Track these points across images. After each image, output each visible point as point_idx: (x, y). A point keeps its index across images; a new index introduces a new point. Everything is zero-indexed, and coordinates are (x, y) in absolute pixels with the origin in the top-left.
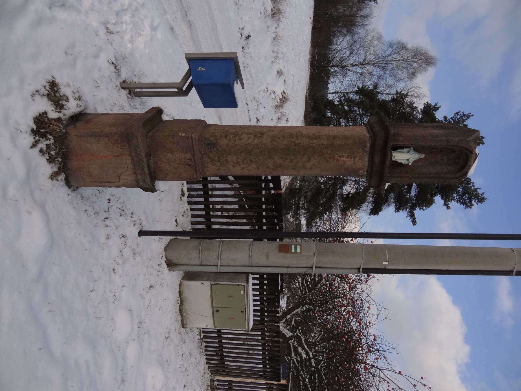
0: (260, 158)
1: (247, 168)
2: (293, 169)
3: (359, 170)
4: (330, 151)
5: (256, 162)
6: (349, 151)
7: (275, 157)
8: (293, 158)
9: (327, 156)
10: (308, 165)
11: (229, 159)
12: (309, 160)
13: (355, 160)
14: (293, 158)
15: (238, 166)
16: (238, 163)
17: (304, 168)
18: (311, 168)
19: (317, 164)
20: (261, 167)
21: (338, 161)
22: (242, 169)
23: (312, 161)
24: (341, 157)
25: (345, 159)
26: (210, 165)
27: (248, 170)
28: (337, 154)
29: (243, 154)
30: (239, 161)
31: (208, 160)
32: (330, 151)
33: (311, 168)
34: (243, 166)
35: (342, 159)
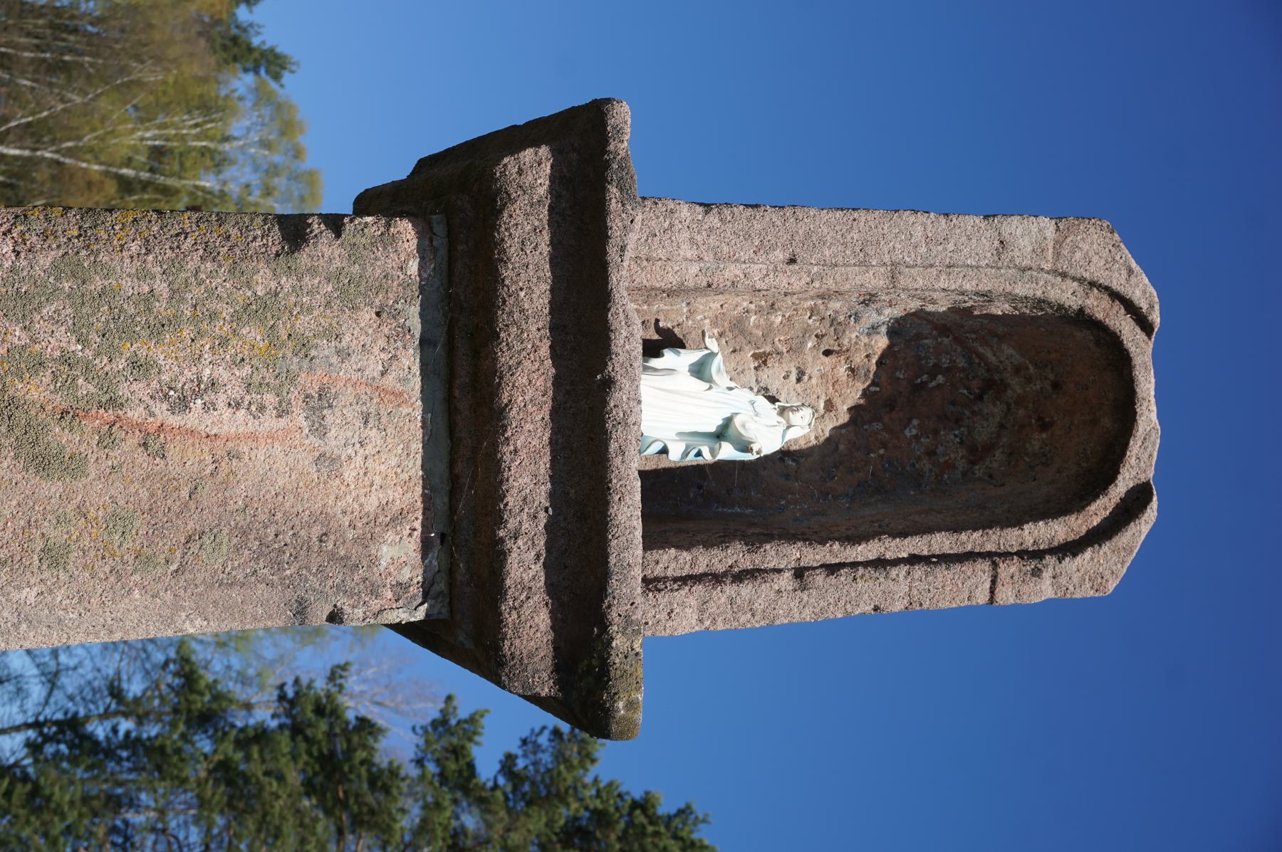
4: (59, 340)
6: (253, 333)
13: (320, 430)
21: (154, 441)
24: (182, 404)
25: (229, 422)
28: (140, 367)
32: (59, 340)
35: (194, 417)
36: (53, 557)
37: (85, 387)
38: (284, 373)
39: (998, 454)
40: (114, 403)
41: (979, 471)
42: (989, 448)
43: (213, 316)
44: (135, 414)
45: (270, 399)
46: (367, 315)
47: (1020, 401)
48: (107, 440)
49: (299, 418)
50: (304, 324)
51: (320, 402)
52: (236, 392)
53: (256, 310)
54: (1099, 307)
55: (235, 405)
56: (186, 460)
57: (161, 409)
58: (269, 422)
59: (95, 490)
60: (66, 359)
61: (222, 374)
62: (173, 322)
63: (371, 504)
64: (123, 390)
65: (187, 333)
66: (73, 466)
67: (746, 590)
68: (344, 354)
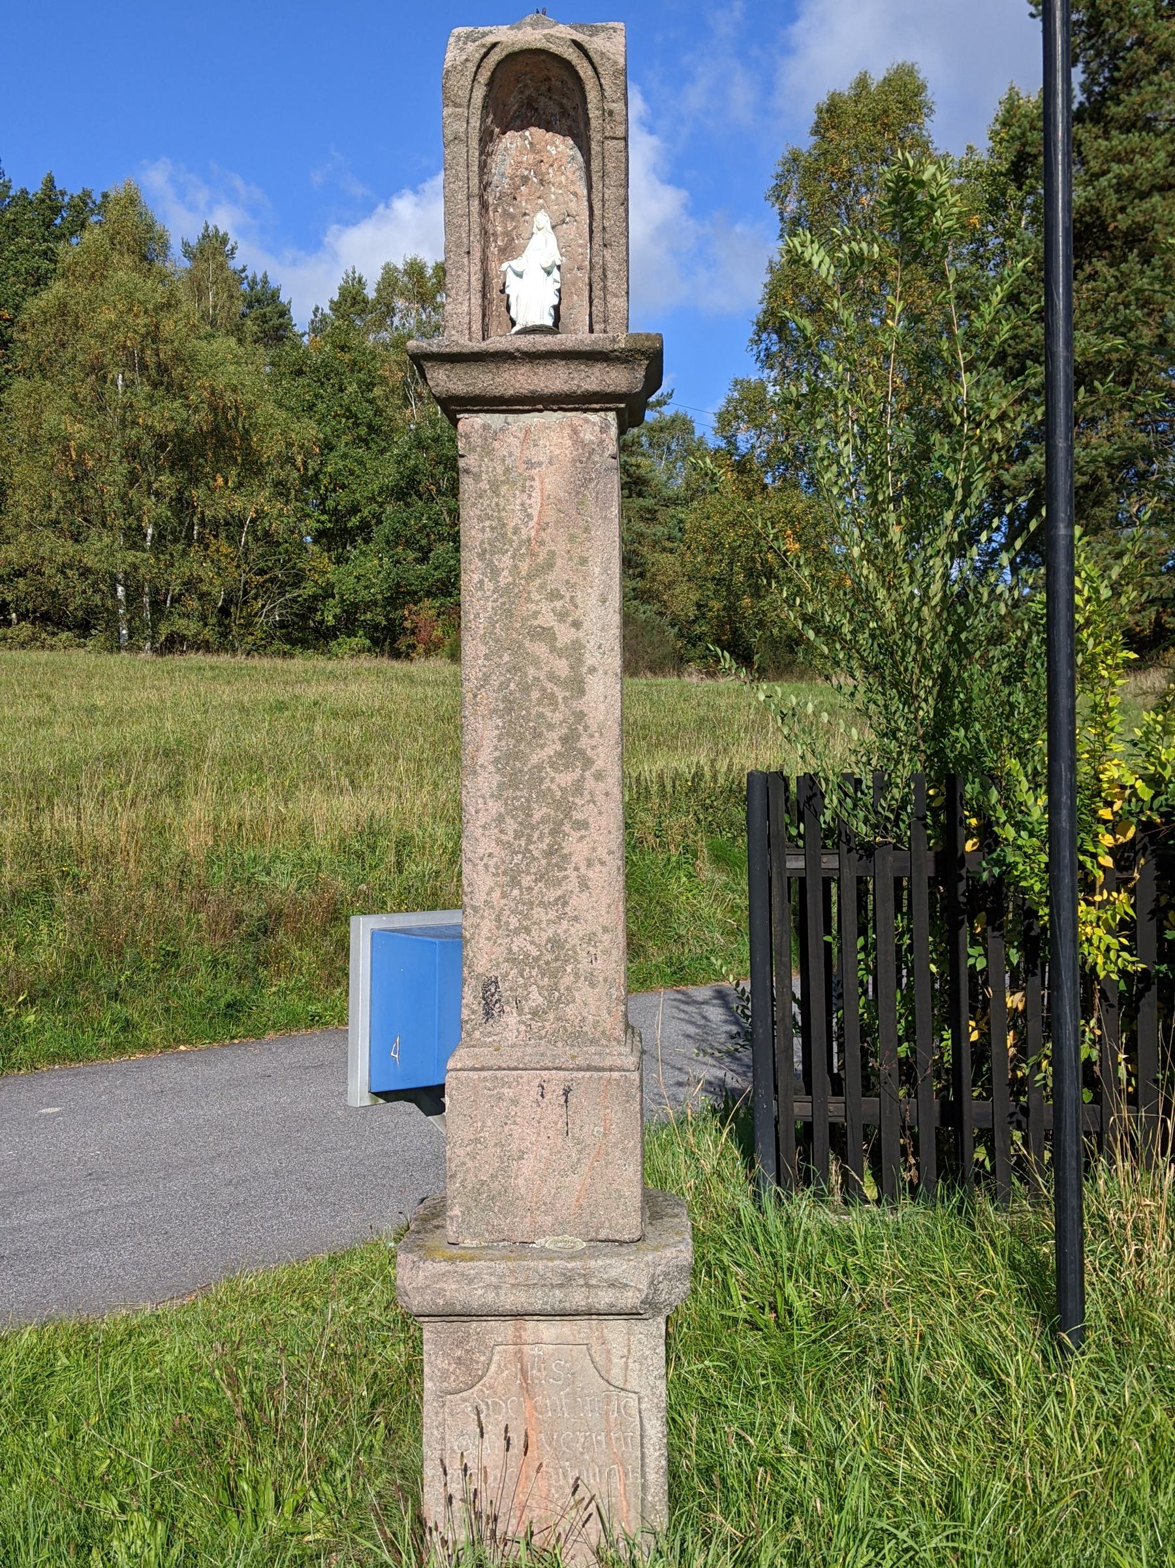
0: (537, 816)
1: (583, 870)
2: (582, 692)
3: (577, 441)
5: (554, 833)
6: (504, 489)
7: (534, 759)
8: (535, 695)
9: (524, 567)
10: (565, 634)
11: (545, 936)
12: (545, 634)
13: (540, 464)
14: (535, 695)
15: (573, 902)
16: (563, 901)
17: (575, 651)
18: (577, 625)
19: (558, 604)
20: (577, 815)
21: (543, 527)
22: (584, 885)
23: (547, 619)
24: (530, 516)
26: (570, 1011)
27: (589, 864)
28: (516, 531)
29: (527, 880)
30: (552, 894)
31: (551, 1016)
33: (577, 625)
34: (573, 884)
35: (534, 512)
36: (584, 561)
37: (523, 550)
38: (516, 479)
39: (565, 101)
40: (529, 540)
41: (572, 113)
42: (561, 106)
43: (497, 504)
44: (533, 533)
45: (528, 483)
46: (496, 444)
47: (537, 89)
48: (542, 543)
49: (535, 471)
50: (500, 470)
51: (530, 464)
52: (525, 496)
53: (495, 487)
54: (484, 76)
55: (530, 496)
56: (551, 515)
57: (531, 524)
58: (536, 484)
59: (561, 547)
60: (513, 558)
61: (518, 501)
62: (500, 519)
63: (569, 443)
64: (524, 537)
65: (504, 514)
66: (552, 554)
67: (610, 274)
68: (511, 454)
